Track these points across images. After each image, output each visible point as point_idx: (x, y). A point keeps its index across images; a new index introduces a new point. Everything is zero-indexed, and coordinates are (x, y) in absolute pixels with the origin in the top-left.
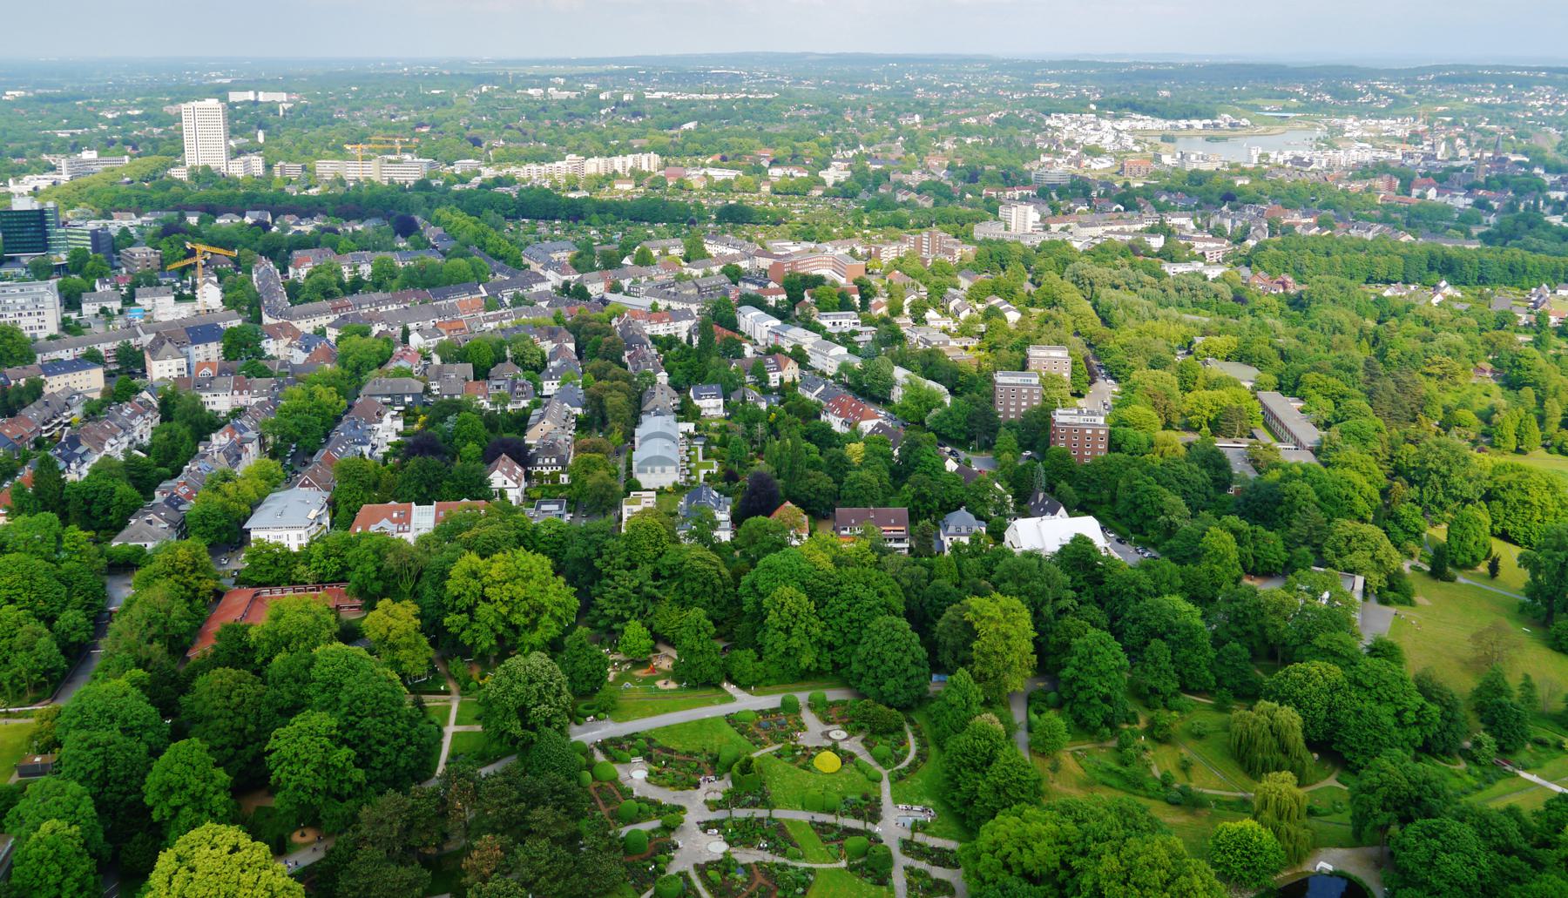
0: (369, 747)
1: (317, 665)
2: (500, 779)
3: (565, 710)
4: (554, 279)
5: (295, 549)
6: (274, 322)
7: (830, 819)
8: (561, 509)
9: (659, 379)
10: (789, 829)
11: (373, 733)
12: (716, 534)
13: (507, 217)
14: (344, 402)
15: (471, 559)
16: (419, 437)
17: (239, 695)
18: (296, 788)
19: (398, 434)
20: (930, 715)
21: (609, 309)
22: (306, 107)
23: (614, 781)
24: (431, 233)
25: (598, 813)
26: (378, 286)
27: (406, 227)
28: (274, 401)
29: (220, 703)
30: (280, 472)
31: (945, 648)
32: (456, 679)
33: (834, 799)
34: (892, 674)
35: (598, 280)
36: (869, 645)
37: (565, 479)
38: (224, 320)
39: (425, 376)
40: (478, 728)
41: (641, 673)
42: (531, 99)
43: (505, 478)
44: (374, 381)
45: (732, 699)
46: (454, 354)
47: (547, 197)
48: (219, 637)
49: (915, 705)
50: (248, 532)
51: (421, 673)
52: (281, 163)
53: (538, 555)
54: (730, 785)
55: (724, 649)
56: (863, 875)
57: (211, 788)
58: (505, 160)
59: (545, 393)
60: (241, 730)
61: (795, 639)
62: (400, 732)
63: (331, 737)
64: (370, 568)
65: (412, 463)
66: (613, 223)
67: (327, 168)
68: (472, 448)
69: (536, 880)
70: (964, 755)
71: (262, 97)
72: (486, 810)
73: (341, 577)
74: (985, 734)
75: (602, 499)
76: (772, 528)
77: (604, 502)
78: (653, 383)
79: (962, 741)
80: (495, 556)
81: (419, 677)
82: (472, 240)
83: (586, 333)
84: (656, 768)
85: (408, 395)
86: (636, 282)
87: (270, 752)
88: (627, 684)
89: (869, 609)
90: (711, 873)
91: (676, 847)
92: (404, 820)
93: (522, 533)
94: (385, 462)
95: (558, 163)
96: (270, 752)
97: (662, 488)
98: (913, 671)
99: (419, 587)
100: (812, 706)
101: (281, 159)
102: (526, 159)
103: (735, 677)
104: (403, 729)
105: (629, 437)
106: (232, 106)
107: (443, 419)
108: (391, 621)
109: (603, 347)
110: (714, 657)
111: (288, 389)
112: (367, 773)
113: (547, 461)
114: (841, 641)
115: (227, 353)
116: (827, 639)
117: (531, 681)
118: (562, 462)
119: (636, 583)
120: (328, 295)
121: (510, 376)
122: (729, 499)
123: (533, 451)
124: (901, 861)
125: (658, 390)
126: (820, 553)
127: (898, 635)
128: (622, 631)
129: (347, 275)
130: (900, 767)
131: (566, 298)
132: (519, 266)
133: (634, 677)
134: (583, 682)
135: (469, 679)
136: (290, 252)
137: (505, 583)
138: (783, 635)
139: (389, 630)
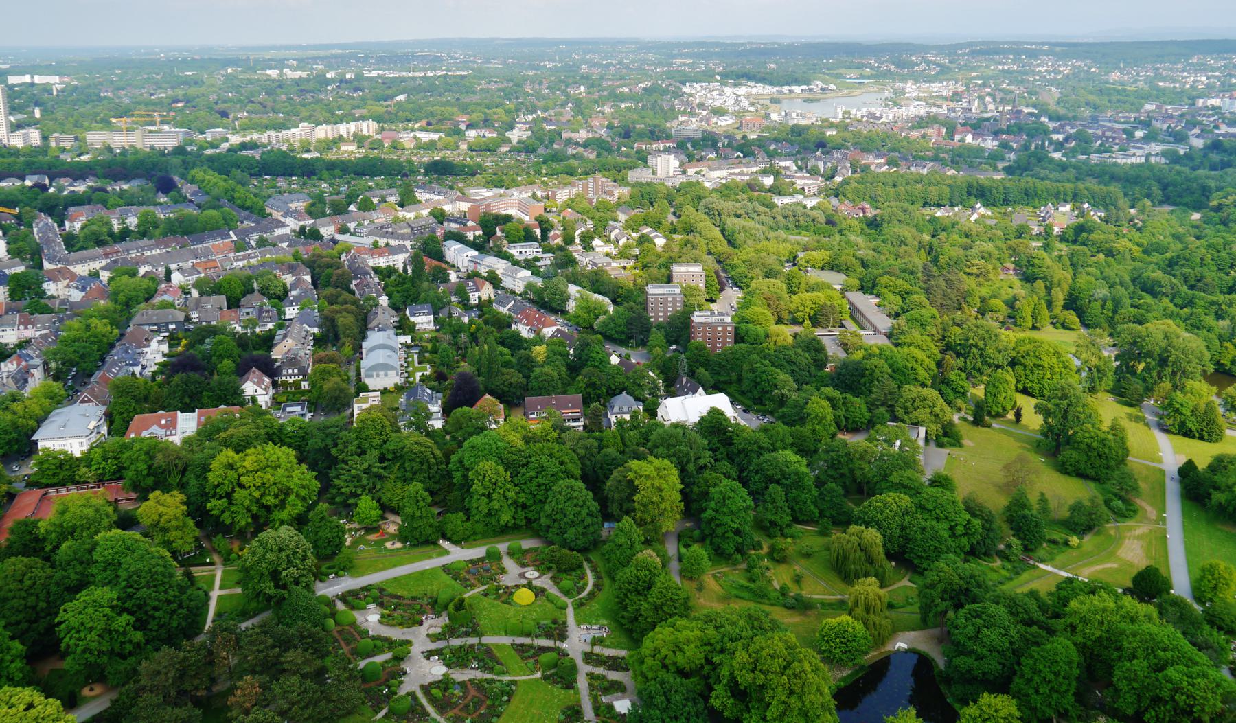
0: (146, 612)
1: (98, 549)
2: (258, 630)
3: (310, 571)
4: (292, 224)
5: (77, 454)
6: (53, 267)
7: (527, 641)
8: (303, 409)
9: (381, 302)
10: (495, 651)
12: (430, 423)
13: (251, 175)
14: (116, 331)
16: (181, 358)
17: (30, 579)
18: (84, 651)
19: (164, 355)
20: (603, 555)
21: (338, 247)
22: (76, 87)
23: (353, 625)
24: (188, 189)
25: (340, 651)
26: (143, 234)
27: (166, 186)
28: (56, 333)
29: (14, 586)
30: (63, 392)
31: (613, 502)
32: (219, 553)
33: (530, 625)
34: (572, 524)
35: (329, 224)
36: (554, 503)
37: (305, 385)
38: (9, 267)
39: (185, 308)
40: (239, 590)
41: (372, 537)
42: (270, 79)
43: (256, 387)
44: (142, 312)
45: (447, 552)
46: (209, 288)
47: (285, 157)
48: (12, 531)
49: (592, 547)
50: (36, 443)
51: (189, 549)
52: (56, 135)
53: (284, 448)
54: (447, 621)
55: (439, 514)
56: (555, 682)
57: (8, 658)
58: (249, 129)
59: (287, 317)
60: (34, 608)
61: (495, 502)
62: (171, 598)
63: (112, 607)
64: (142, 466)
65: (177, 378)
66: (340, 177)
67: (96, 138)
68: (227, 364)
69: (290, 709)
70: (630, 583)
71: (38, 79)
72: (246, 657)
73: (118, 475)
74: (645, 566)
75: (336, 400)
76: (474, 416)
77: (338, 402)
78: (376, 305)
79: (628, 572)
80: (248, 451)
81: (188, 553)
82: (223, 194)
83: (320, 267)
84: (387, 612)
85: (172, 323)
86: (360, 224)
87: (60, 623)
88: (362, 547)
89: (552, 475)
90: (434, 691)
91: (405, 673)
93: (271, 431)
94: (153, 379)
95: (293, 130)
96: (60, 623)
97: (386, 389)
98: (589, 521)
99: (184, 480)
100: (511, 554)
101: (55, 131)
102: (266, 128)
103: (449, 535)
104: (175, 596)
105: (358, 349)
106: (11, 87)
107: (202, 342)
108: (162, 509)
109: (334, 278)
110: (431, 521)
111: (67, 322)
112: (145, 635)
113: (290, 371)
114: (532, 501)
115: (13, 295)
116: (521, 500)
117: (281, 550)
118: (303, 372)
119: (366, 465)
120: (100, 243)
121: (257, 304)
122: (440, 395)
123: (278, 364)
124: (584, 668)
125: (380, 311)
126: (513, 433)
127: (576, 494)
128: (356, 505)
129: (116, 226)
130: (581, 596)
131: (303, 239)
132: (263, 214)
133: (367, 541)
134: (325, 548)
135: (231, 552)
136: (66, 208)
138: (486, 500)
139: (160, 516)
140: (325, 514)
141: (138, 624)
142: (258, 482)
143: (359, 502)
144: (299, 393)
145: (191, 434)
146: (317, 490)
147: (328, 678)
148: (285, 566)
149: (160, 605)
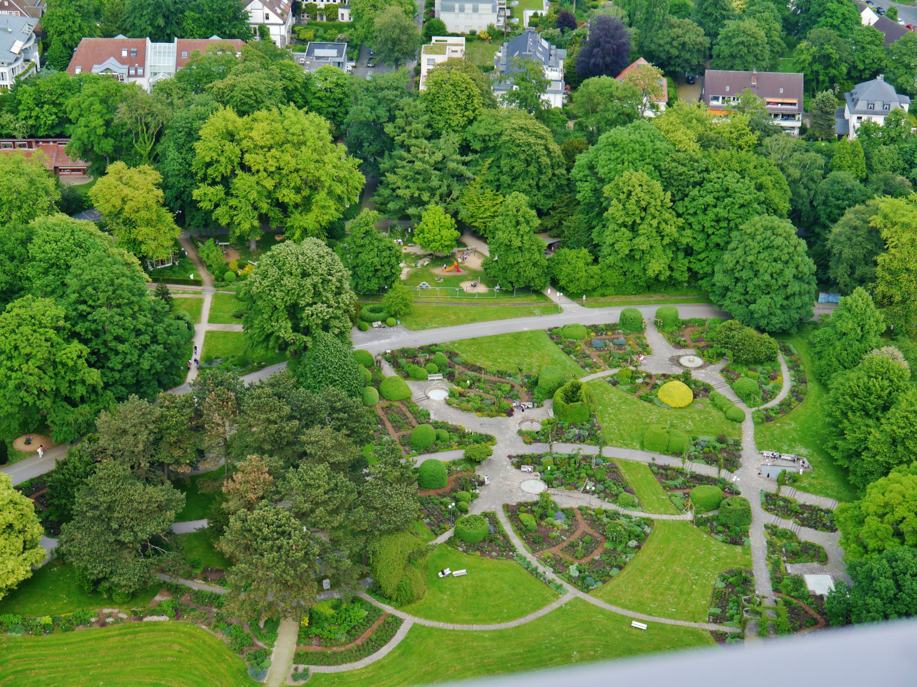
0: (105, 343)
1: (36, 240)
2: (268, 390)
3: (347, 311)
7: (675, 462)
8: (340, 54)
10: (622, 470)
11: (109, 327)
12: (544, 97)
15: (226, 117)
18: (18, 388)
23: (406, 401)
25: (386, 438)
31: (839, 261)
33: (681, 438)
34: (767, 290)
36: (739, 252)
40: (238, 327)
41: (440, 271)
43: (267, 10)
45: (557, 309)
49: (794, 330)
51: (165, 257)
53: (312, 115)
54: (551, 414)
55: (550, 246)
56: (713, 531)
61: (642, 238)
62: (143, 328)
63: (58, 329)
64: (97, 121)
69: (312, 511)
70: (854, 396)
72: (250, 426)
74: (884, 373)
75: (394, 44)
76: (618, 94)
79: (854, 378)
80: (257, 114)
84: (459, 389)
88: (424, 284)
89: (742, 206)
90: (525, 517)
91: (482, 483)
92: (151, 432)
93: (291, 86)
97: (473, 33)
98: (795, 287)
99: (159, 149)
100: (660, 324)
103: (562, 283)
104: (147, 325)
108: (126, 191)
110: (537, 256)
112: (103, 374)
114: (702, 244)
116: (684, 241)
117: (305, 275)
119: (438, 156)
122: (563, 52)
124: (762, 518)
126: (683, 129)
127: (779, 241)
128: (420, 218)
130: (770, 405)
133: (432, 275)
134: (369, 279)
135: (224, 269)
137: (270, 148)
138: (628, 234)
139: (124, 201)
140: (372, 226)
141: (93, 359)
142: (272, 165)
143: (424, 214)
144: (335, 27)
145: (167, 77)
146: (360, 187)
147: (368, 475)
148: (311, 301)
149: (125, 334)
